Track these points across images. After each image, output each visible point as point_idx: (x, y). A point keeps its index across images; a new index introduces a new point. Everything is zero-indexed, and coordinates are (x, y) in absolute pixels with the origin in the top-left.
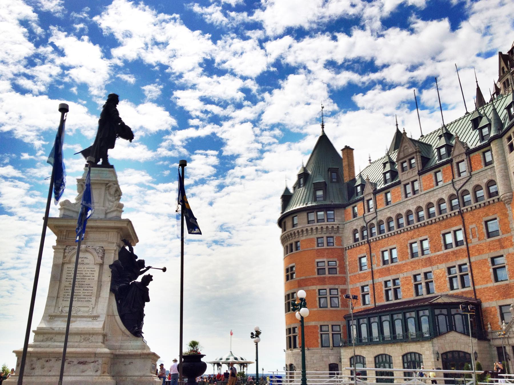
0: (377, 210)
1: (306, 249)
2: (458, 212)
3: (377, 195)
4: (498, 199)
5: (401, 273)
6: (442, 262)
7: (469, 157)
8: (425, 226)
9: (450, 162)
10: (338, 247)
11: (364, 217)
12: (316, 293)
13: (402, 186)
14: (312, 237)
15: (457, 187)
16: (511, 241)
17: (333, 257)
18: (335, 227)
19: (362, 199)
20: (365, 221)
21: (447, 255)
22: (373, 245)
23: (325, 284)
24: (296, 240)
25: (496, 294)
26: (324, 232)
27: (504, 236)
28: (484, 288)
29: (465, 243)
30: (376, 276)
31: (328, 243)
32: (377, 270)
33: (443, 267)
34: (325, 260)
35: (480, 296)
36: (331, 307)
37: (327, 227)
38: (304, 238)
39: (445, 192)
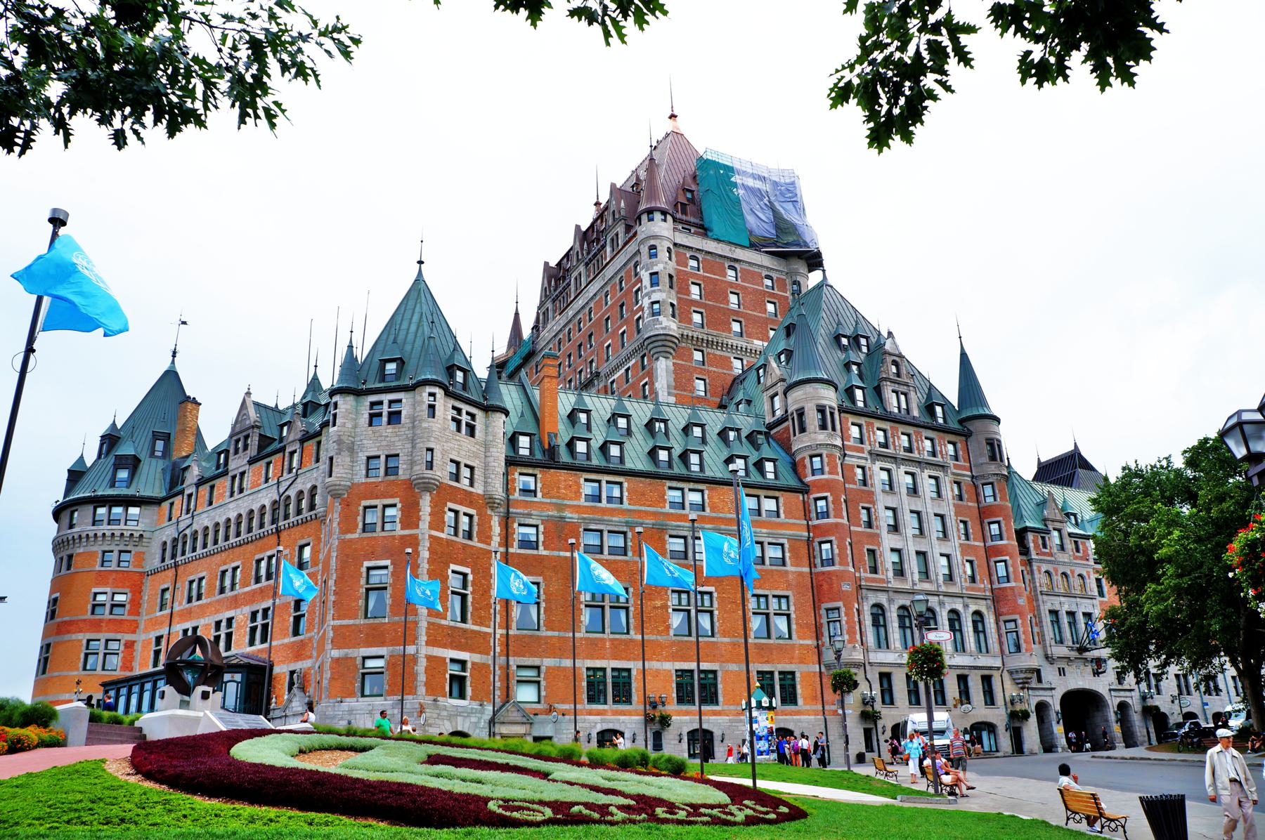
8: (240, 545)
9: (283, 449)
12: (82, 645)
13: (229, 478)
14: (94, 549)
15: (281, 490)
17: (123, 587)
18: (137, 534)
22: (181, 569)
23: (99, 631)
24: (69, 552)
30: (176, 619)
31: (119, 561)
33: (247, 610)
37: (122, 534)
38: (81, 550)
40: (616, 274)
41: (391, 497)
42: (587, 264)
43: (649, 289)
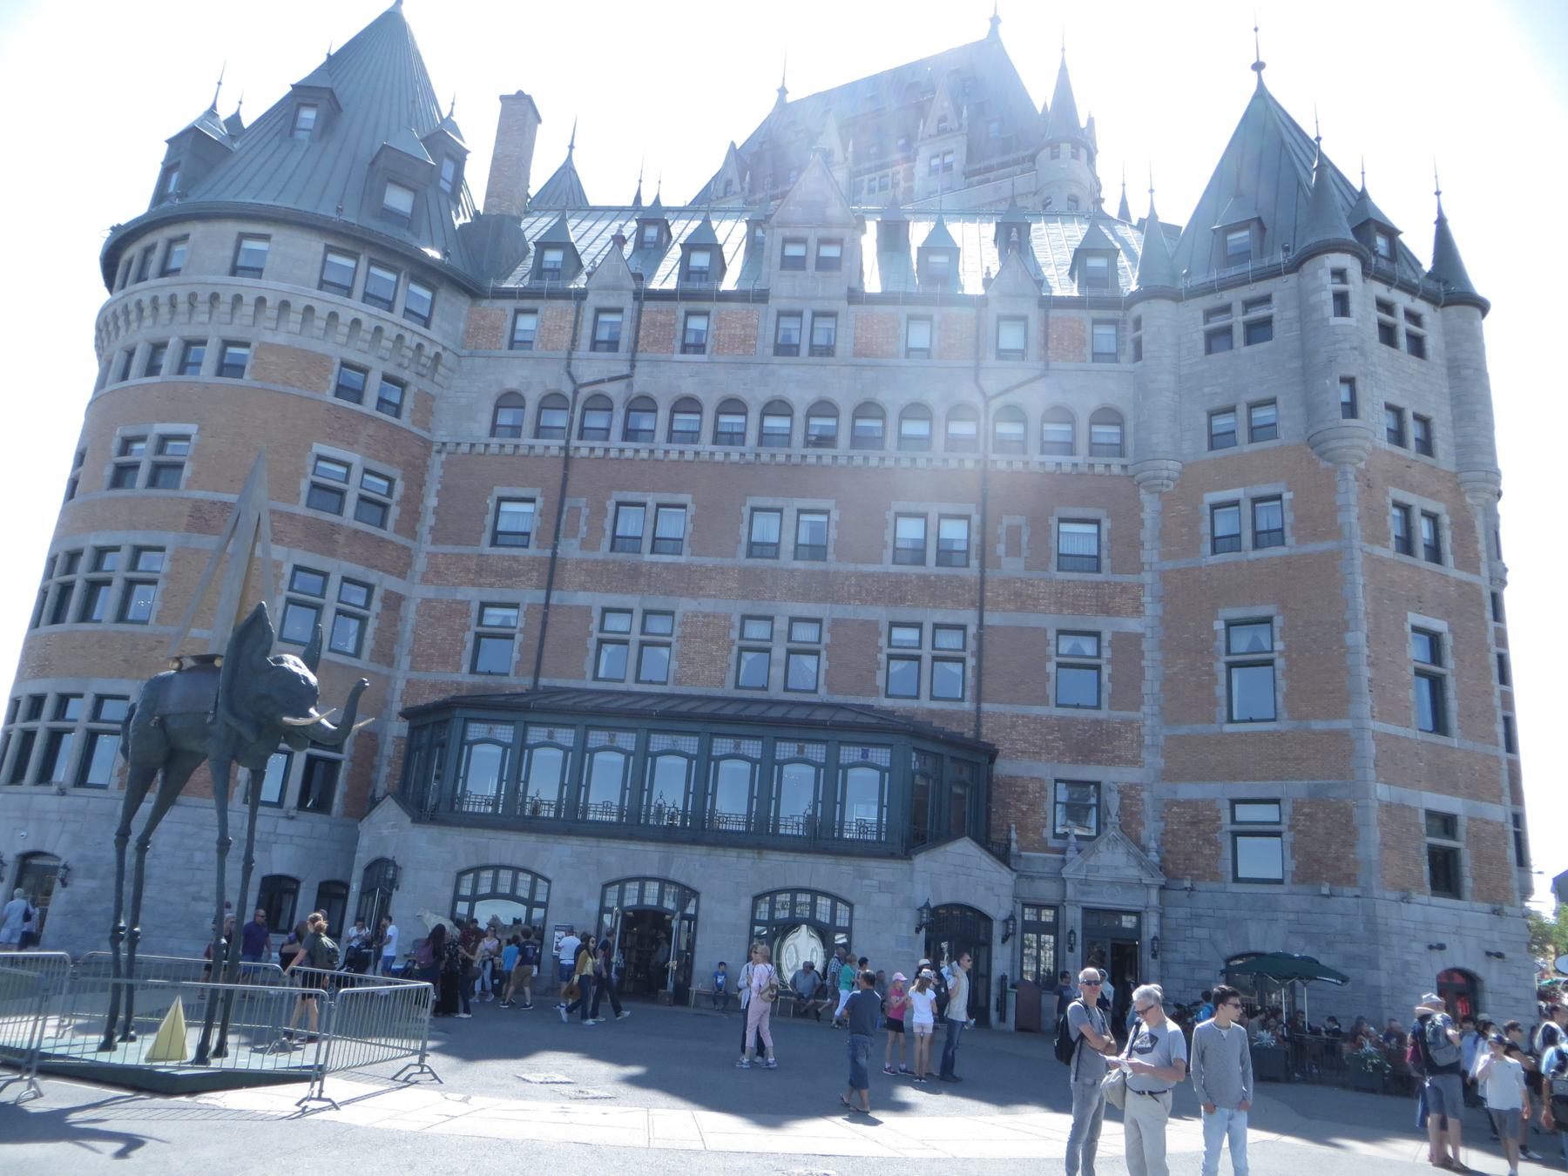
0: (639, 356)
2: (977, 461)
3: (649, 306)
4: (1124, 467)
5: (694, 596)
6: (876, 601)
7: (1047, 316)
10: (415, 429)
11: (569, 359)
12: (279, 577)
16: (1137, 599)
18: (430, 350)
20: (569, 374)
21: (898, 583)
23: (331, 553)
24: (231, 333)
25: (1053, 741)
26: (381, 352)
27: (1118, 578)
28: (1012, 717)
29: (974, 563)
34: (355, 458)
35: (995, 737)
38: (280, 339)
41: (1433, 496)
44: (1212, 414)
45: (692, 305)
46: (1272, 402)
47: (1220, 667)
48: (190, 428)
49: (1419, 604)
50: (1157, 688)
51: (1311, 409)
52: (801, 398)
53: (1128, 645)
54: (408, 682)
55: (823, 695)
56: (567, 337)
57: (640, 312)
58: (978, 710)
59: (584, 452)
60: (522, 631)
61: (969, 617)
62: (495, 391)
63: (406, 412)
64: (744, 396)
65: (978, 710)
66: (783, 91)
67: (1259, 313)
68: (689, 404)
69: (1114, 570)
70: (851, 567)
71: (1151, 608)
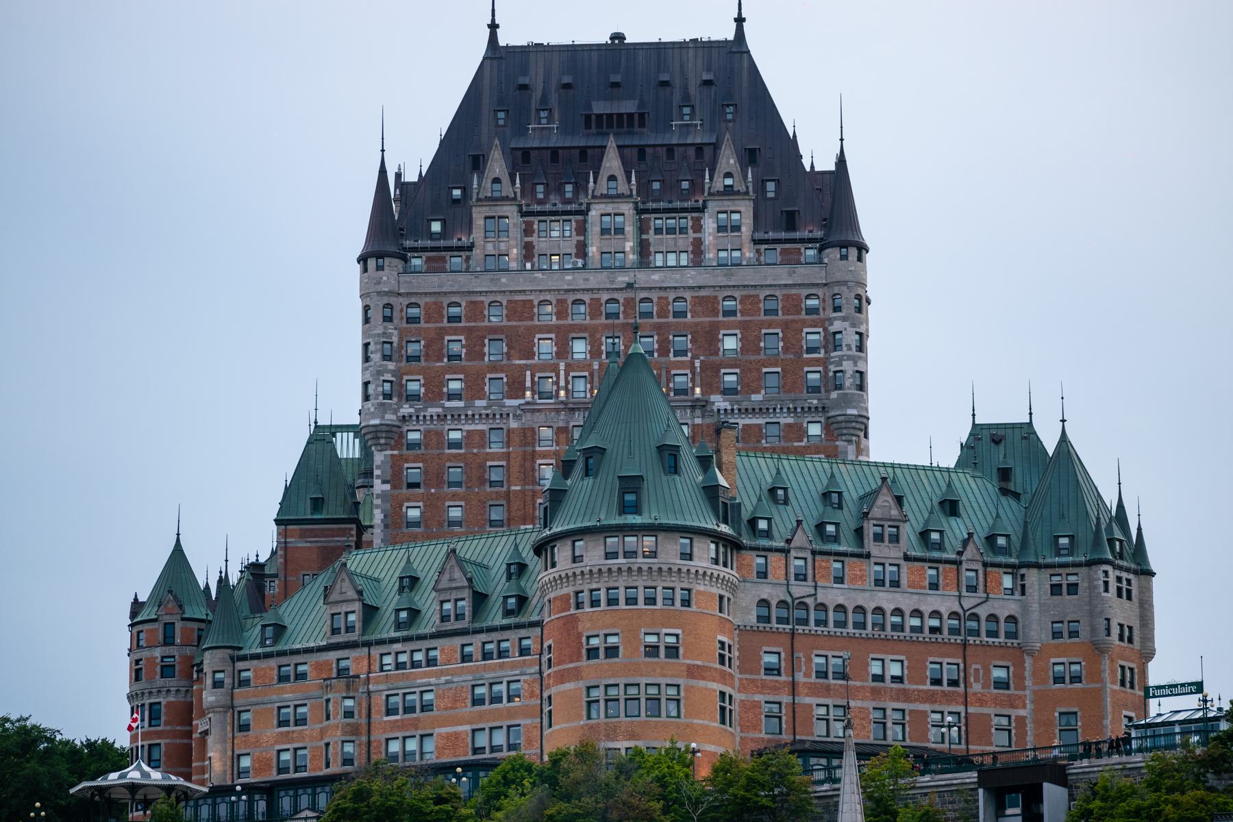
0: (819, 584)
1: (706, 611)
4: (1019, 644)
6: (926, 702)
7: (985, 571)
11: (788, 585)
16: (1024, 701)
19: (785, 551)
21: (934, 693)
23: (726, 684)
24: (685, 585)
29: (962, 685)
32: (806, 683)
36: (626, 716)
38: (702, 588)
39: (945, 604)
40: (762, 286)
42: (640, 212)
43: (854, 352)
44: (1053, 623)
45: (836, 558)
46: (1078, 621)
47: (1057, 731)
48: (679, 631)
49: (1126, 707)
50: (1032, 738)
51: (1093, 630)
52: (889, 607)
53: (1021, 720)
54: (741, 738)
55: (908, 742)
56: (783, 572)
57: (814, 560)
58: (967, 748)
59: (800, 631)
60: (785, 715)
61: (961, 709)
62: (757, 599)
63: (731, 614)
64: (865, 606)
65: (967, 748)
66: (493, 27)
67: (1072, 579)
68: (840, 608)
69: (1015, 689)
70: (915, 687)
71: (1029, 706)
